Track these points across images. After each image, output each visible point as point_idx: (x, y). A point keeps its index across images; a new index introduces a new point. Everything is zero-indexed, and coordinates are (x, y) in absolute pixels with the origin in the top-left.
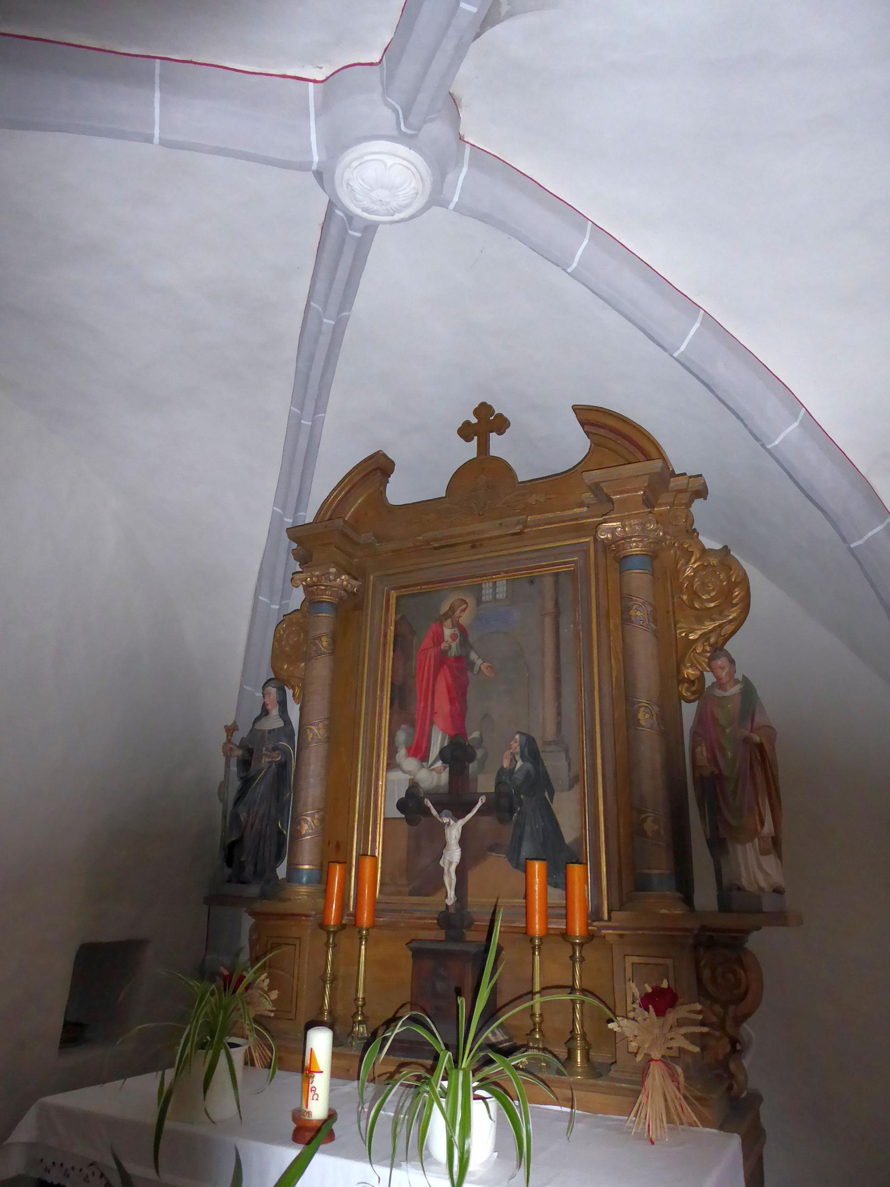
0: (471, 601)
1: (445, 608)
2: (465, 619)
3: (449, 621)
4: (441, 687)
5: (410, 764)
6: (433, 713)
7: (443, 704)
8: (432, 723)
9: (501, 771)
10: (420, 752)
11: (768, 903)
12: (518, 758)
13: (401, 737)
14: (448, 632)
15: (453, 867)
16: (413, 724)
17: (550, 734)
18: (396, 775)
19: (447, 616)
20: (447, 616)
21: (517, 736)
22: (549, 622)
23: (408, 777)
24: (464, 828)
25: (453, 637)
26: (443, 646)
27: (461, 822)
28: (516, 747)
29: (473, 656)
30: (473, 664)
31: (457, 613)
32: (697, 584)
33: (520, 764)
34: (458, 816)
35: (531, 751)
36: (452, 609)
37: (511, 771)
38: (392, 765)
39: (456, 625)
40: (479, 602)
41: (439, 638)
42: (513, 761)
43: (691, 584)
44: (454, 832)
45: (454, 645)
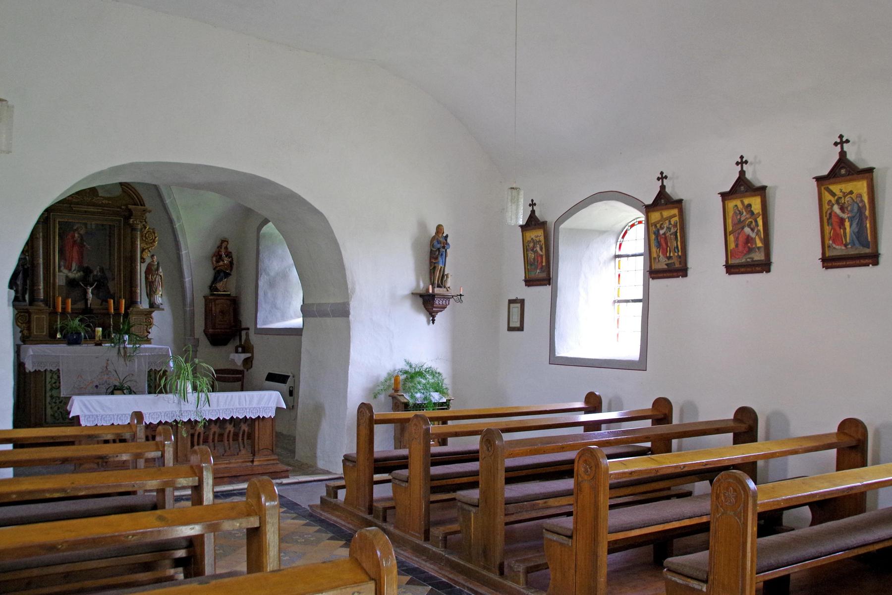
1: (75, 228)
2: (82, 232)
3: (76, 232)
5: (66, 271)
6: (72, 258)
7: (75, 255)
8: (72, 261)
11: (161, 307)
12: (99, 272)
13: (62, 263)
14: (76, 235)
15: (91, 299)
16: (66, 260)
17: (108, 267)
18: (61, 274)
21: (99, 267)
22: (107, 238)
23: (65, 274)
24: (92, 290)
25: (79, 237)
26: (75, 239)
27: (91, 288)
28: (98, 269)
29: (85, 243)
30: (85, 246)
31: (80, 230)
32: (147, 236)
33: (99, 274)
34: (91, 286)
35: (102, 270)
37: (97, 275)
38: (60, 271)
39: (79, 233)
40: (86, 228)
41: (73, 237)
43: (146, 236)
45: (79, 239)
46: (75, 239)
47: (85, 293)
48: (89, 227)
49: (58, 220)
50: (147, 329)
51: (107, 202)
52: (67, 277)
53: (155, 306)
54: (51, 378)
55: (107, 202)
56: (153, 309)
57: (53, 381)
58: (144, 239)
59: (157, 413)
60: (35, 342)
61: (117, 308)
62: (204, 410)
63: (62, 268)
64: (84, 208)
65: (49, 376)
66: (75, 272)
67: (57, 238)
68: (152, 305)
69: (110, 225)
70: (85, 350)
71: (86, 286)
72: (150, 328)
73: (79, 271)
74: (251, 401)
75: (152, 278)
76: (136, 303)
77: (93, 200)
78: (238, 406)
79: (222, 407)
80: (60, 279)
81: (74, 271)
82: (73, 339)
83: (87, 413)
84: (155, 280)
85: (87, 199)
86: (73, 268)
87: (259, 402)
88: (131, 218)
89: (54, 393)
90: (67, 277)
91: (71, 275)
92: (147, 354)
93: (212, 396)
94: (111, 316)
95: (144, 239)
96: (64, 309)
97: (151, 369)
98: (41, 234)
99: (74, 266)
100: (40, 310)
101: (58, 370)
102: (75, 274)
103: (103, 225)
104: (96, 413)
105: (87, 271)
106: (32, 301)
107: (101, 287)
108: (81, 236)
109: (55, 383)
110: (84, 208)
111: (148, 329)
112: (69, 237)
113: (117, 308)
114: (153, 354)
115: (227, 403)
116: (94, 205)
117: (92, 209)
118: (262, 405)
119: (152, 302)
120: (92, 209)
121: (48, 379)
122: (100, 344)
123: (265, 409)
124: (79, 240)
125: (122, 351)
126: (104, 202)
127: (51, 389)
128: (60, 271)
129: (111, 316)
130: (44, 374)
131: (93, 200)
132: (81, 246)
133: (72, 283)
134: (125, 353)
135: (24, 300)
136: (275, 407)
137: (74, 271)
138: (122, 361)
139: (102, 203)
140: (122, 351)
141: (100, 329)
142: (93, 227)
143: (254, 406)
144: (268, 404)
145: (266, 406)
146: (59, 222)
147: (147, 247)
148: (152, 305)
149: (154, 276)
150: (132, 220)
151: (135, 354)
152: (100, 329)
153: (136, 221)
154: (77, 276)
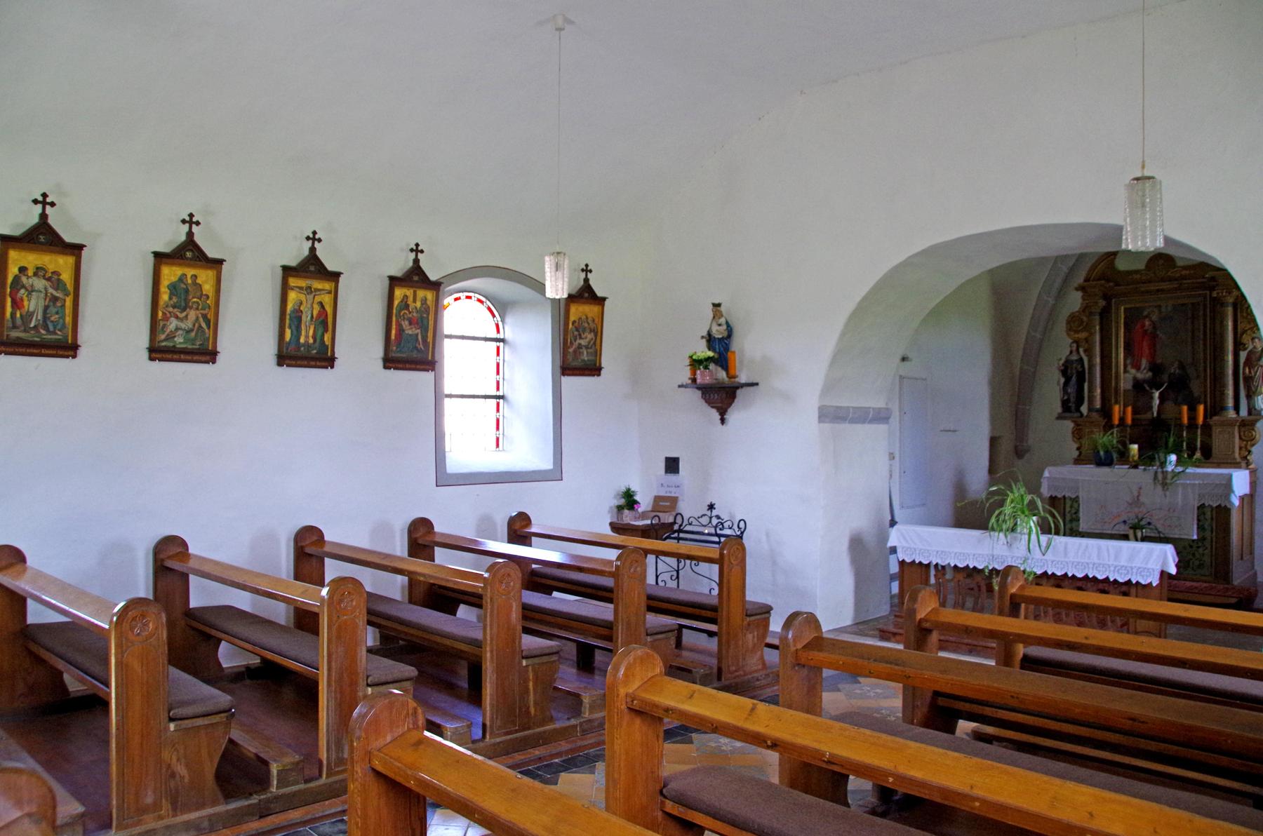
0: (1156, 311)
1: (1145, 313)
2: (1154, 318)
3: (1147, 319)
4: (1145, 344)
5: (1133, 371)
7: (1146, 350)
9: (1171, 374)
10: (1138, 368)
13: (1128, 361)
14: (1147, 323)
18: (1127, 375)
19: (1146, 317)
20: (1146, 317)
24: (1160, 394)
26: (1146, 328)
27: (1159, 391)
28: (1176, 365)
29: (1158, 332)
30: (1158, 335)
33: (1177, 371)
34: (1157, 390)
35: (1182, 366)
36: (1149, 314)
37: (1174, 374)
39: (1151, 321)
40: (1160, 312)
41: (1143, 326)
42: (1175, 371)
44: (1157, 394)
46: (1146, 328)
47: (1152, 398)
48: (1163, 309)
49: (1122, 308)
50: (1246, 445)
51: (1188, 272)
52: (1135, 379)
53: (1253, 411)
54: (1071, 507)
55: (1188, 272)
56: (1252, 418)
57: (1073, 511)
58: (1245, 315)
59: (964, 554)
60: (1085, 462)
61: (1193, 418)
62: (1046, 560)
63: (1129, 368)
64: (1152, 287)
65: (1068, 503)
66: (1145, 371)
67: (1122, 330)
68: (1251, 410)
69: (1193, 304)
70: (1120, 471)
71: (1151, 389)
72: (1253, 445)
73: (1150, 370)
74: (1116, 557)
75: (1250, 372)
76: (1224, 408)
77: (1169, 274)
78: (1096, 561)
79: (1071, 559)
80: (1125, 383)
81: (1144, 369)
82: (1105, 462)
83: (905, 544)
84: (1255, 375)
85: (1161, 273)
86: (1143, 367)
87: (1131, 558)
88: (1215, 290)
89: (1074, 524)
90: (1135, 379)
91: (1140, 376)
92: (1197, 482)
93: (1057, 541)
94: (1185, 428)
95: (1245, 315)
96: (1122, 420)
97: (1204, 504)
98: (1098, 328)
99: (1144, 363)
100: (1092, 422)
101: (1077, 497)
102: (1144, 375)
103: (1183, 305)
104: (913, 546)
105: (1156, 368)
106: (1090, 410)
107: (1178, 388)
108: (1153, 323)
109: (1076, 513)
110: (1152, 287)
111: (1248, 447)
112: (1139, 326)
113: (1193, 418)
114: (1205, 482)
115: (1080, 554)
116: (1170, 279)
117: (1165, 286)
118: (1137, 563)
119: (1251, 406)
120: (1165, 286)
121: (1068, 509)
122: (1136, 467)
123: (1140, 571)
124: (1150, 329)
125: (1160, 476)
126: (1184, 272)
127: (1071, 521)
128: (1125, 371)
129: (1185, 428)
130: (1062, 501)
131: (1169, 274)
132: (1154, 337)
133: (1138, 385)
134: (1165, 478)
135: (1078, 410)
136: (1159, 570)
137: (1144, 369)
138: (1159, 488)
139: (1181, 275)
140: (1160, 476)
141: (1135, 447)
142: (1169, 309)
143: (1122, 564)
144: (1147, 563)
145: (1143, 566)
146: (1125, 309)
147: (1248, 327)
148: (1251, 410)
149: (1253, 367)
150: (1215, 292)
151: (1174, 480)
152: (1135, 447)
153: (1222, 293)
154: (1147, 376)
